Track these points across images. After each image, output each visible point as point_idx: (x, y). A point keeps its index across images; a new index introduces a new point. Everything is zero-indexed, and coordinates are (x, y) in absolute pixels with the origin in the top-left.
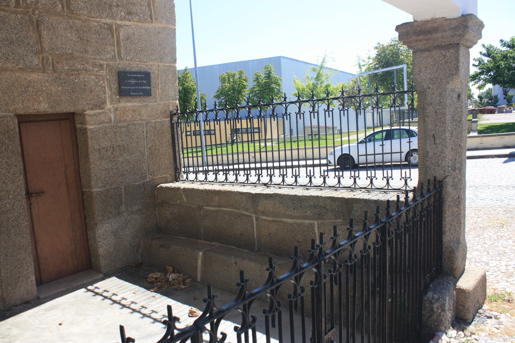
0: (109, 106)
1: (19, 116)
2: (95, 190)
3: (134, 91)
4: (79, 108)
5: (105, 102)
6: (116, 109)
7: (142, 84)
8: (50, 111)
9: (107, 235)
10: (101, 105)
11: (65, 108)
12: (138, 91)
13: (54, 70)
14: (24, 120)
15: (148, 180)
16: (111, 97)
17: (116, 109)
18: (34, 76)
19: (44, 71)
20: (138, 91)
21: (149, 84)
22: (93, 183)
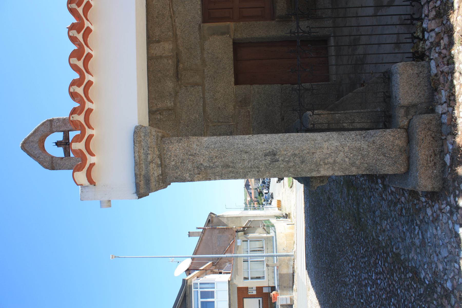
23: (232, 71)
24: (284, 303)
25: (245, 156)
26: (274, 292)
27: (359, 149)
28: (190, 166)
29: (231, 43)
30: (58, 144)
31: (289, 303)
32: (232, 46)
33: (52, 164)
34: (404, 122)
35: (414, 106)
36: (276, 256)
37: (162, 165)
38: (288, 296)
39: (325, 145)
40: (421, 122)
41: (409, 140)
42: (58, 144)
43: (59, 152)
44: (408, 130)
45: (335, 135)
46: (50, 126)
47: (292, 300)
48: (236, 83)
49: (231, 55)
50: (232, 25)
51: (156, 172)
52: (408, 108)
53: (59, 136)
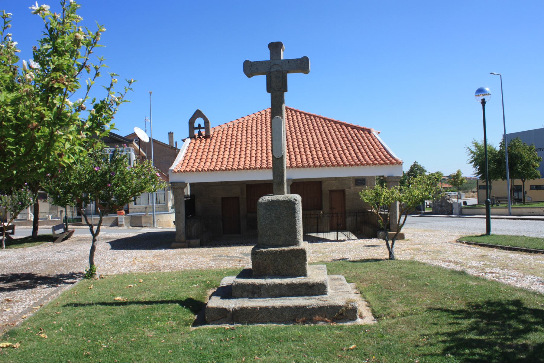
9: (349, 221)
10: (350, 188)
11: (341, 188)
14: (331, 191)
21: (365, 182)
24: (119, 220)
26: (124, 212)
30: (199, 125)
31: (119, 223)
33: (191, 122)
34: (187, 241)
36: (153, 214)
37: (177, 188)
38: (124, 223)
42: (199, 125)
43: (196, 125)
44: (185, 242)
45: (184, 226)
46: (207, 122)
47: (121, 226)
48: (223, 198)
50: (245, 196)
51: (175, 187)
53: (203, 125)
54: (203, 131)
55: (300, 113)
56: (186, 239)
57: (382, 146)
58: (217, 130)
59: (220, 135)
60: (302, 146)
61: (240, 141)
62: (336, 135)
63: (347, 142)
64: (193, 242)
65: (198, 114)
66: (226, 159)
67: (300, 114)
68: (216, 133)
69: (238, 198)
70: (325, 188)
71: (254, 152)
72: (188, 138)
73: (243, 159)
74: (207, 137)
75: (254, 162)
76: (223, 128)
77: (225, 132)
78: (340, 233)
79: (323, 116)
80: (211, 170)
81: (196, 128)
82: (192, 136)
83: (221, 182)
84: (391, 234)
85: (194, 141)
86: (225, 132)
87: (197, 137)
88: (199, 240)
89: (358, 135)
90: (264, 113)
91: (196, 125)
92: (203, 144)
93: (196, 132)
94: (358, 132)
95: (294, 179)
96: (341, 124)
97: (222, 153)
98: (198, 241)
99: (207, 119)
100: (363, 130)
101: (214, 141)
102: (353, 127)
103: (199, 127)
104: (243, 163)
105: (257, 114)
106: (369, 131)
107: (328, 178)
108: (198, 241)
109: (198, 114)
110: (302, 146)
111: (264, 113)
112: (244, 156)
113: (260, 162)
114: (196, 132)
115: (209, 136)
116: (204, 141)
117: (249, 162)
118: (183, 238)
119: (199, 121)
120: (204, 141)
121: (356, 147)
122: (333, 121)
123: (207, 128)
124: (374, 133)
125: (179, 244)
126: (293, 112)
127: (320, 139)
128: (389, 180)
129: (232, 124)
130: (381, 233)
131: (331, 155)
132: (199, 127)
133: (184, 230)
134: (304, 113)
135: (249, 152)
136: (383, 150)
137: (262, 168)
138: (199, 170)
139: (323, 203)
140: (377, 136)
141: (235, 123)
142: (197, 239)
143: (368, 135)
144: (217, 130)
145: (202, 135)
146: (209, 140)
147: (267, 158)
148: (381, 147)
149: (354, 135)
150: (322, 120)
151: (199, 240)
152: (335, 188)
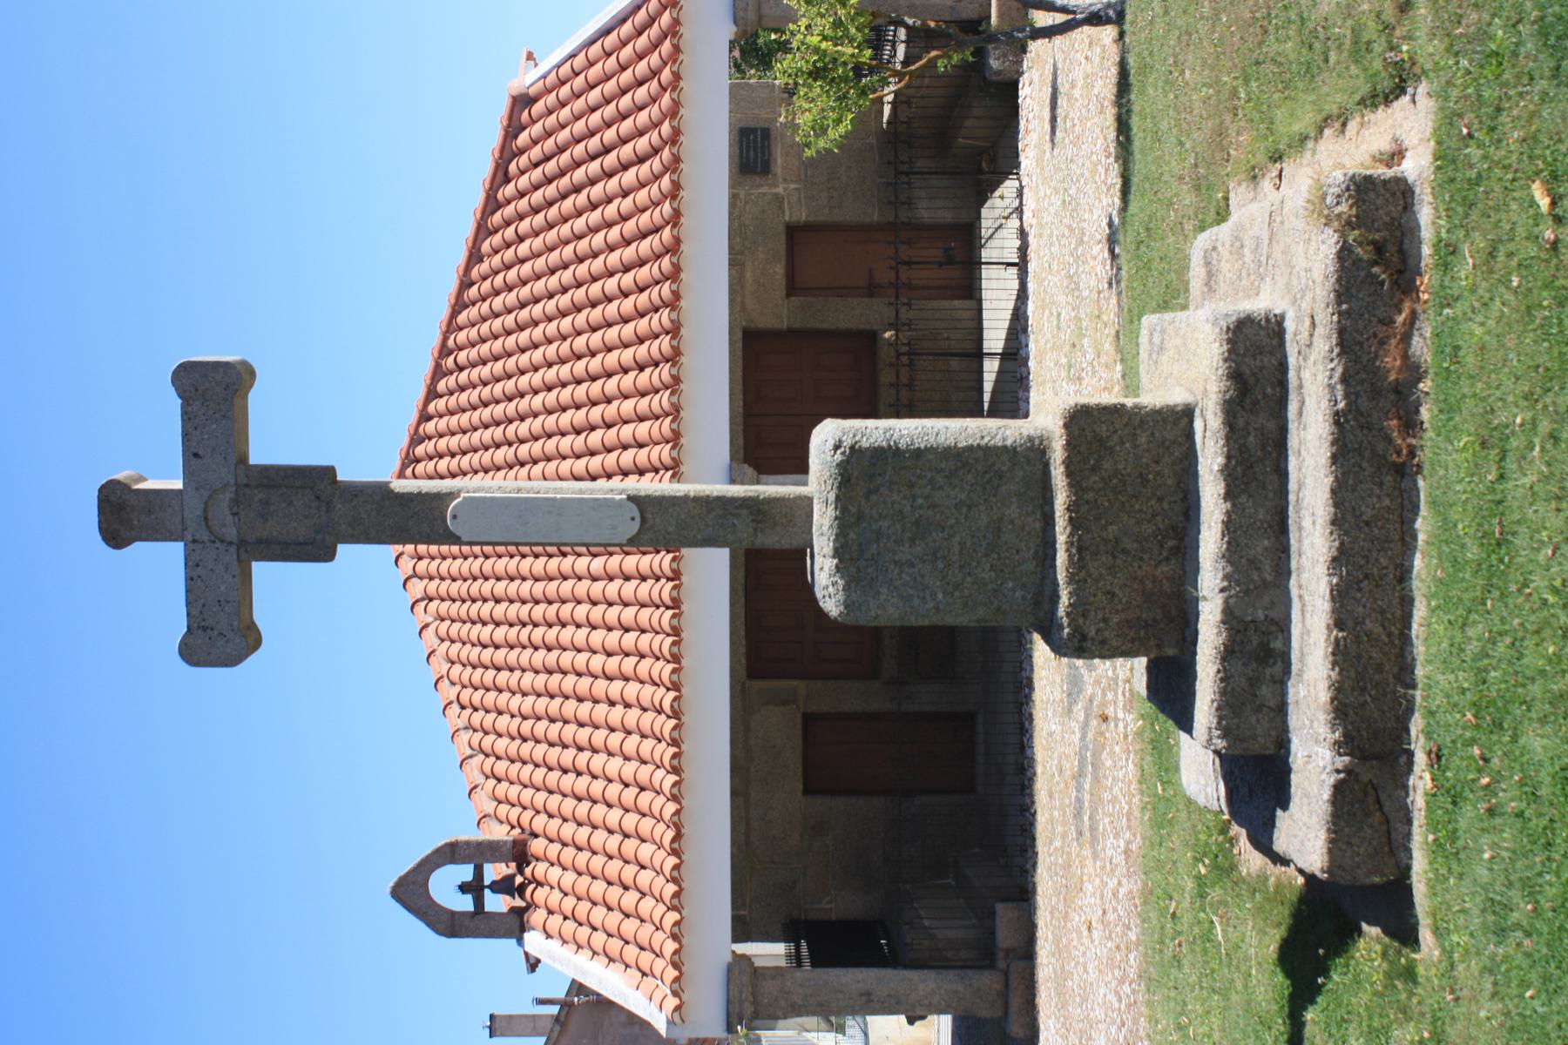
0: (780, 190)
1: (788, 295)
2: (876, 218)
3: (763, 153)
4: (782, 228)
5: (776, 195)
6: (785, 180)
7: (755, 142)
8: (784, 263)
9: (931, 209)
10: (779, 200)
11: (781, 245)
12: (763, 146)
13: (741, 253)
14: (792, 289)
15: (874, 141)
16: (771, 186)
17: (785, 180)
18: (748, 276)
19: (743, 265)
20: (763, 146)
21: (753, 130)
22: (868, 220)
23: (800, 773)
25: (840, 996)
27: (956, 992)
28: (783, 1003)
29: (799, 720)
30: (464, 888)
32: (800, 727)
34: (1002, 964)
35: (1014, 950)
37: (755, 1003)
39: (921, 987)
40: (1017, 967)
41: (1007, 984)
42: (464, 888)
43: (465, 903)
44: (1006, 973)
45: (932, 974)
46: (451, 853)
48: (807, 791)
49: (799, 742)
50: (800, 685)
51: (748, 1009)
52: (1008, 952)
53: (466, 872)
54: (494, 871)
55: (425, 417)
56: (991, 966)
57: (591, 42)
58: (490, 807)
59: (514, 791)
60: (579, 417)
61: (544, 701)
62: (536, 255)
63: (568, 205)
64: (1005, 937)
65: (411, 892)
66: (629, 770)
67: (430, 418)
68: (503, 808)
69: (809, 719)
70: (777, 313)
71: (597, 637)
72: (520, 942)
73: (632, 689)
74: (520, 854)
75: (647, 637)
76: (481, 779)
77: (501, 767)
78: (985, 255)
79: (444, 311)
80: (678, 837)
81: (479, 902)
82: (515, 925)
83: (734, 793)
84: (1001, 16)
85: (537, 917)
86: (501, 767)
87: (519, 903)
88: (1000, 908)
89: (536, 153)
90: (417, 587)
91: (465, 903)
92: (555, 873)
93: (497, 903)
94: (522, 152)
95: (732, 458)
96: (483, 230)
97: (597, 787)
98: (1005, 913)
99: (438, 851)
100: (513, 128)
101: (540, 822)
102: (501, 175)
103: (474, 888)
104: (649, 689)
105: (421, 616)
106: (522, 101)
107: (732, 301)
108: (1005, 913)
109: (411, 892)
110: (579, 417)
111: (417, 587)
112: (617, 685)
113: (646, 612)
114: (497, 903)
115: (515, 842)
116: (540, 869)
117: (647, 662)
118: (987, 981)
119: (446, 887)
120: (540, 869)
121: (594, 167)
122: (468, 269)
123: (477, 853)
124: (528, 79)
125: (1016, 1001)
126: (420, 450)
127: (551, 328)
128: (752, 16)
129: (465, 736)
130: (994, 63)
131: (627, 280)
132: (474, 888)
133: (951, 974)
134: (427, 401)
135: (597, 662)
136: (611, 40)
137: (676, 604)
138: (677, 895)
139: (843, 325)
140: (545, 66)
141: (461, 723)
142: (992, 914)
143: (538, 107)
144: (490, 807)
145: (511, 878)
146: (537, 846)
147: (627, 578)
148: (595, 50)
149: (537, 174)
150: (462, 318)
151: (1000, 908)
152: (779, 269)
